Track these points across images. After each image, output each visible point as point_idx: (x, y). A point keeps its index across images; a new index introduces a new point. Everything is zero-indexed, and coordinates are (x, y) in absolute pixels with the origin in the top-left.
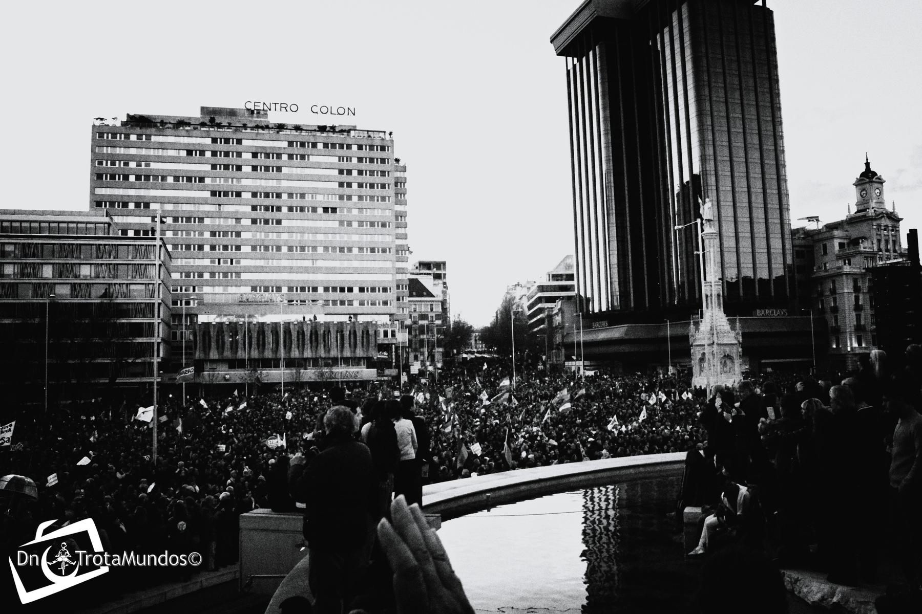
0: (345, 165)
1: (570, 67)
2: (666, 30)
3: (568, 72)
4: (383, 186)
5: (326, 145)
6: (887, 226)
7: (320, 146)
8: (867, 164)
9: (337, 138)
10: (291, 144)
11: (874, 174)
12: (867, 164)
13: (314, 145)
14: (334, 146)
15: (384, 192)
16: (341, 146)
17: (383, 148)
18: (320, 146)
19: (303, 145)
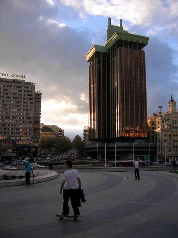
0: (20, 93)
1: (90, 65)
2: (116, 57)
3: (89, 67)
4: (31, 99)
5: (14, 87)
6: (176, 116)
7: (13, 87)
8: (172, 98)
9: (17, 85)
10: (4, 86)
11: (173, 101)
12: (172, 98)
13: (11, 86)
14: (17, 87)
15: (31, 101)
16: (19, 87)
17: (32, 88)
18: (13, 87)
19: (8, 86)
